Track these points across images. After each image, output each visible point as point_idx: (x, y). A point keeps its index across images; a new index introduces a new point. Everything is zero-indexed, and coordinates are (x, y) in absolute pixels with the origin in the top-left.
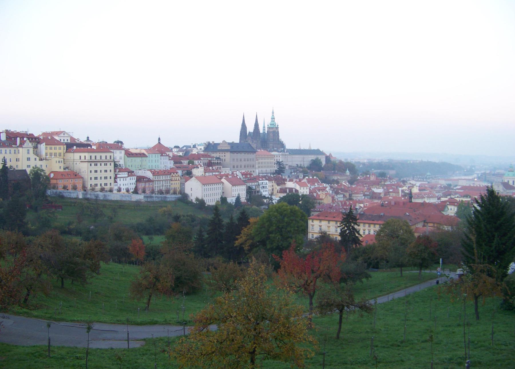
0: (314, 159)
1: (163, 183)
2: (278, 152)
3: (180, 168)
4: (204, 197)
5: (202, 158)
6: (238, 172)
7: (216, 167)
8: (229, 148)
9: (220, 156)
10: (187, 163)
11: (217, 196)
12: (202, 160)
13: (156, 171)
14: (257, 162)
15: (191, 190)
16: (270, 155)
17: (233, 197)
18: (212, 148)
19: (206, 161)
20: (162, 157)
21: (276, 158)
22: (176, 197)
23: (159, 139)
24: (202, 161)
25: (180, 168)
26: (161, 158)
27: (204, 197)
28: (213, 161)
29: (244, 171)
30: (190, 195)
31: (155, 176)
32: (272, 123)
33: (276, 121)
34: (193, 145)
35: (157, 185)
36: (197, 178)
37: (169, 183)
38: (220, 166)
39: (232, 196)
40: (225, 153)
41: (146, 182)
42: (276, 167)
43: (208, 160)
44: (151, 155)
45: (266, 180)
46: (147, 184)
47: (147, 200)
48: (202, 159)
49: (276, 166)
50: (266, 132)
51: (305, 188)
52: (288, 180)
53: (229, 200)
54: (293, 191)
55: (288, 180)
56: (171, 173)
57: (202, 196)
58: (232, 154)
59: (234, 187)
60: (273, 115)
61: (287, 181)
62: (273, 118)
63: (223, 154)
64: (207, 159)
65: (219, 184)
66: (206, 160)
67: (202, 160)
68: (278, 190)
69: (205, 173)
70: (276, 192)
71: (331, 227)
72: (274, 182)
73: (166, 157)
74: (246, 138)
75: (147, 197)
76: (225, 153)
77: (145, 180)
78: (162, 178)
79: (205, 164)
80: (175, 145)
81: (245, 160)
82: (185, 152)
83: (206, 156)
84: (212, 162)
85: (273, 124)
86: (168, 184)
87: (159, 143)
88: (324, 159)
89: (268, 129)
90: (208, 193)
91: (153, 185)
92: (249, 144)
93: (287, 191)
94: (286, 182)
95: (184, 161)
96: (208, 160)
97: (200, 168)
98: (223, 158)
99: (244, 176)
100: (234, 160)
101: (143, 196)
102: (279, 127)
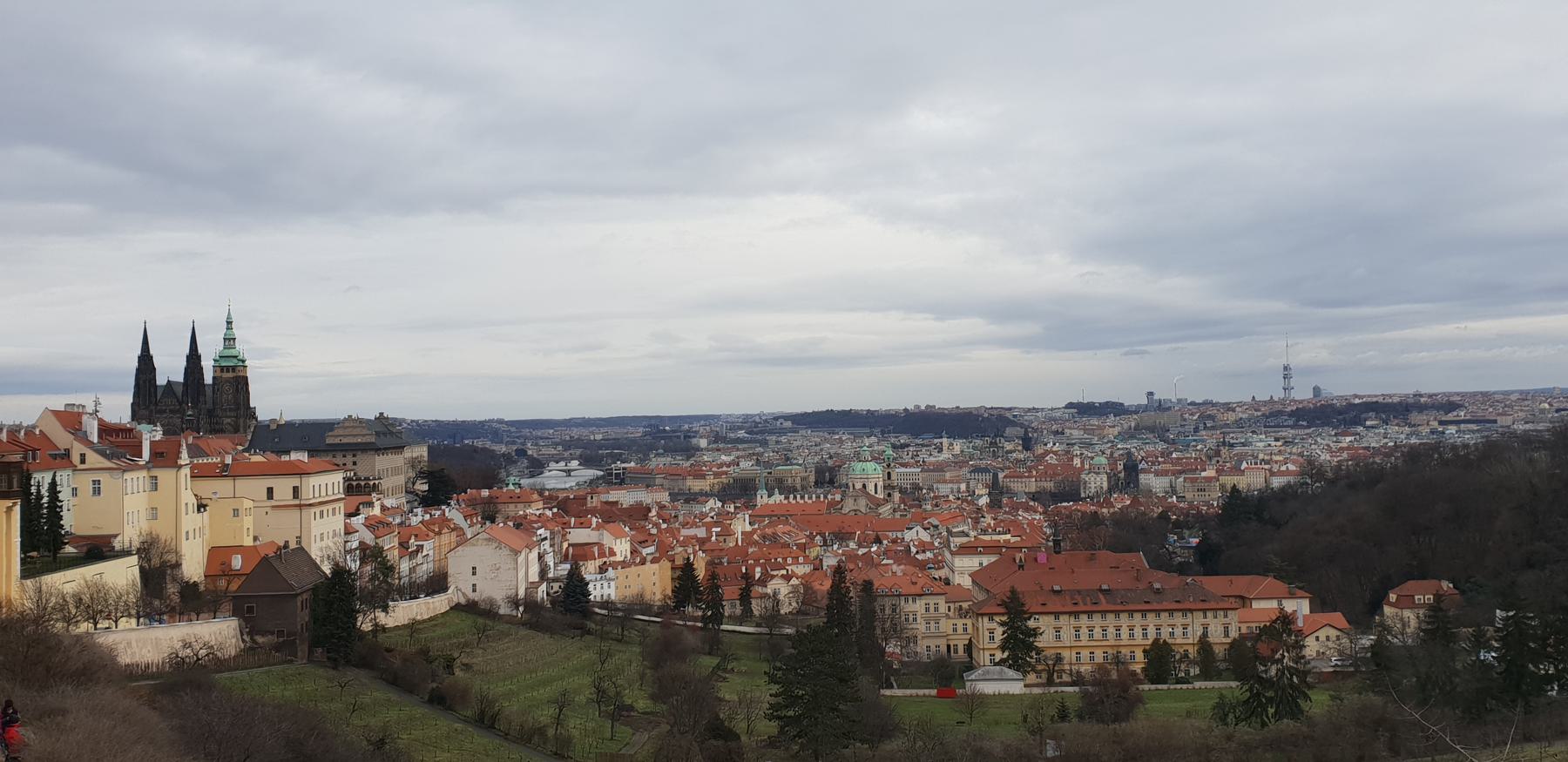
89: (215, 371)
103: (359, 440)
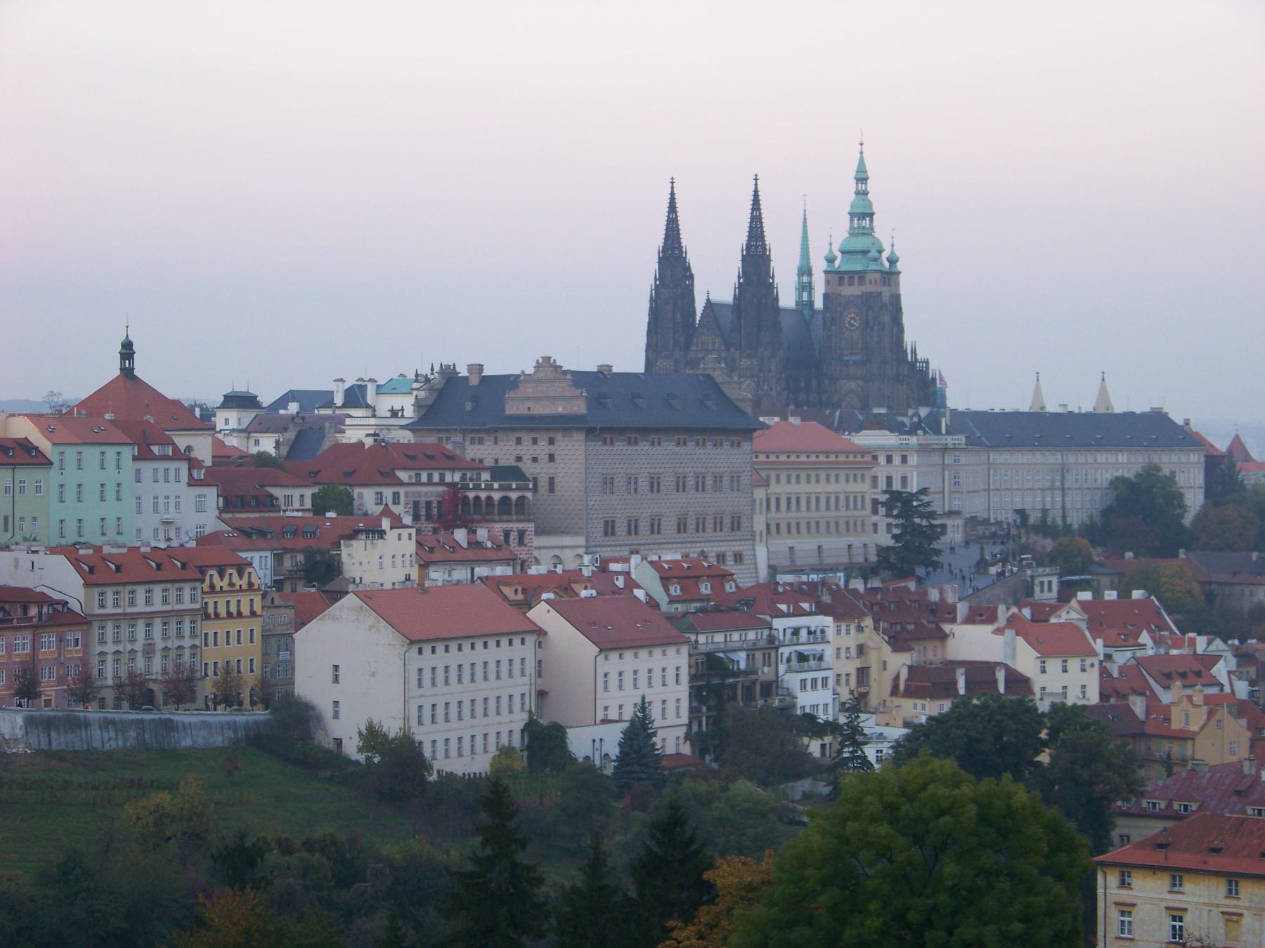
0: (1129, 473)
1: (148, 634)
2: (899, 429)
3: (263, 534)
4: (420, 723)
5: (405, 469)
6: (635, 559)
7: (498, 528)
8: (579, 407)
9: (519, 459)
10: (308, 504)
11: (505, 716)
12: (401, 484)
13: (105, 559)
14: (760, 494)
15: (336, 680)
16: (847, 453)
17: (605, 721)
18: (468, 407)
19: (433, 493)
20: (147, 468)
21: (881, 471)
22: (234, 726)
23: (127, 351)
24: (402, 490)
25: (263, 534)
26: (138, 471)
27: (420, 723)
28: (477, 487)
29: (678, 557)
30: (328, 711)
31: (97, 590)
32: (860, 243)
33: (883, 230)
34: (347, 385)
35: (110, 648)
36: (374, 599)
37: (193, 635)
38: (521, 525)
39: (600, 716)
40: (551, 441)
41: (37, 628)
42: (882, 527)
43: (442, 482)
44: (71, 453)
45: (822, 610)
46: (49, 641)
47: (44, 746)
48: (403, 476)
49: (881, 520)
50: (819, 304)
51: (1074, 664)
52: (962, 609)
53: (580, 743)
54: (995, 682)
55: (962, 609)
56: (202, 570)
57: (406, 718)
58: (597, 446)
59: (614, 656)
60: (865, 193)
61: (953, 621)
62: (862, 215)
63: (543, 448)
64: (436, 478)
65: (517, 641)
66: (430, 483)
67: (401, 484)
68: (897, 678)
69: (424, 566)
70: (887, 686)
71: (1248, 919)
72: (868, 622)
73: (172, 465)
74: (688, 346)
75: (49, 724)
76: (551, 441)
77: (33, 611)
78: (148, 602)
79: (423, 512)
80: (228, 391)
81: (680, 485)
82: (291, 435)
83: (432, 458)
84: (471, 495)
85: (865, 252)
86: (187, 642)
87: (128, 372)
88: (1198, 477)
89: (828, 282)
90: (441, 694)
91: (86, 646)
92: (710, 378)
93: (955, 683)
94: (947, 628)
95: (288, 492)
96: (442, 482)
97: (391, 535)
98: (542, 470)
99: (675, 590)
100: (608, 481)
101: (19, 720)
102: (900, 266)
103: (560, 410)
